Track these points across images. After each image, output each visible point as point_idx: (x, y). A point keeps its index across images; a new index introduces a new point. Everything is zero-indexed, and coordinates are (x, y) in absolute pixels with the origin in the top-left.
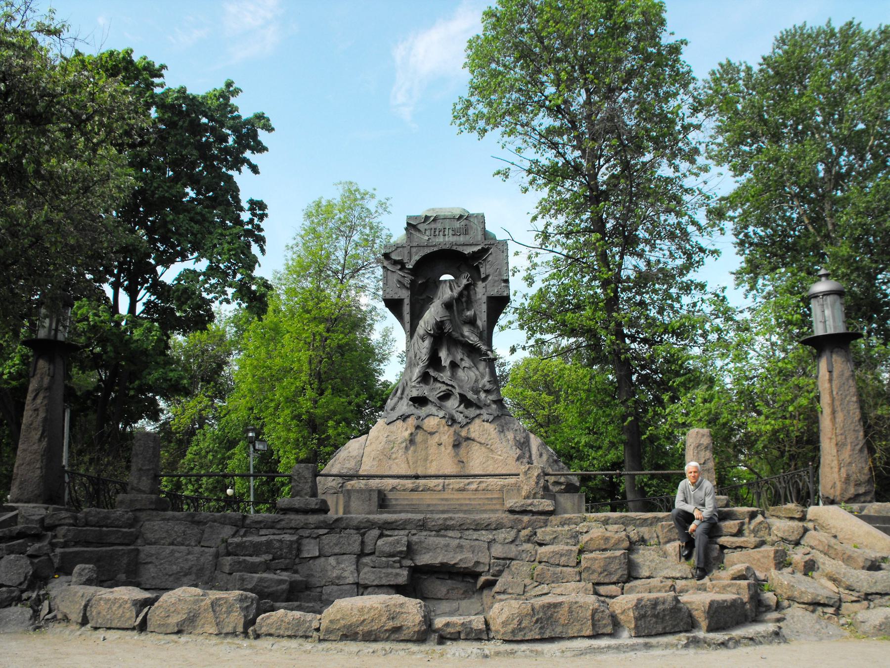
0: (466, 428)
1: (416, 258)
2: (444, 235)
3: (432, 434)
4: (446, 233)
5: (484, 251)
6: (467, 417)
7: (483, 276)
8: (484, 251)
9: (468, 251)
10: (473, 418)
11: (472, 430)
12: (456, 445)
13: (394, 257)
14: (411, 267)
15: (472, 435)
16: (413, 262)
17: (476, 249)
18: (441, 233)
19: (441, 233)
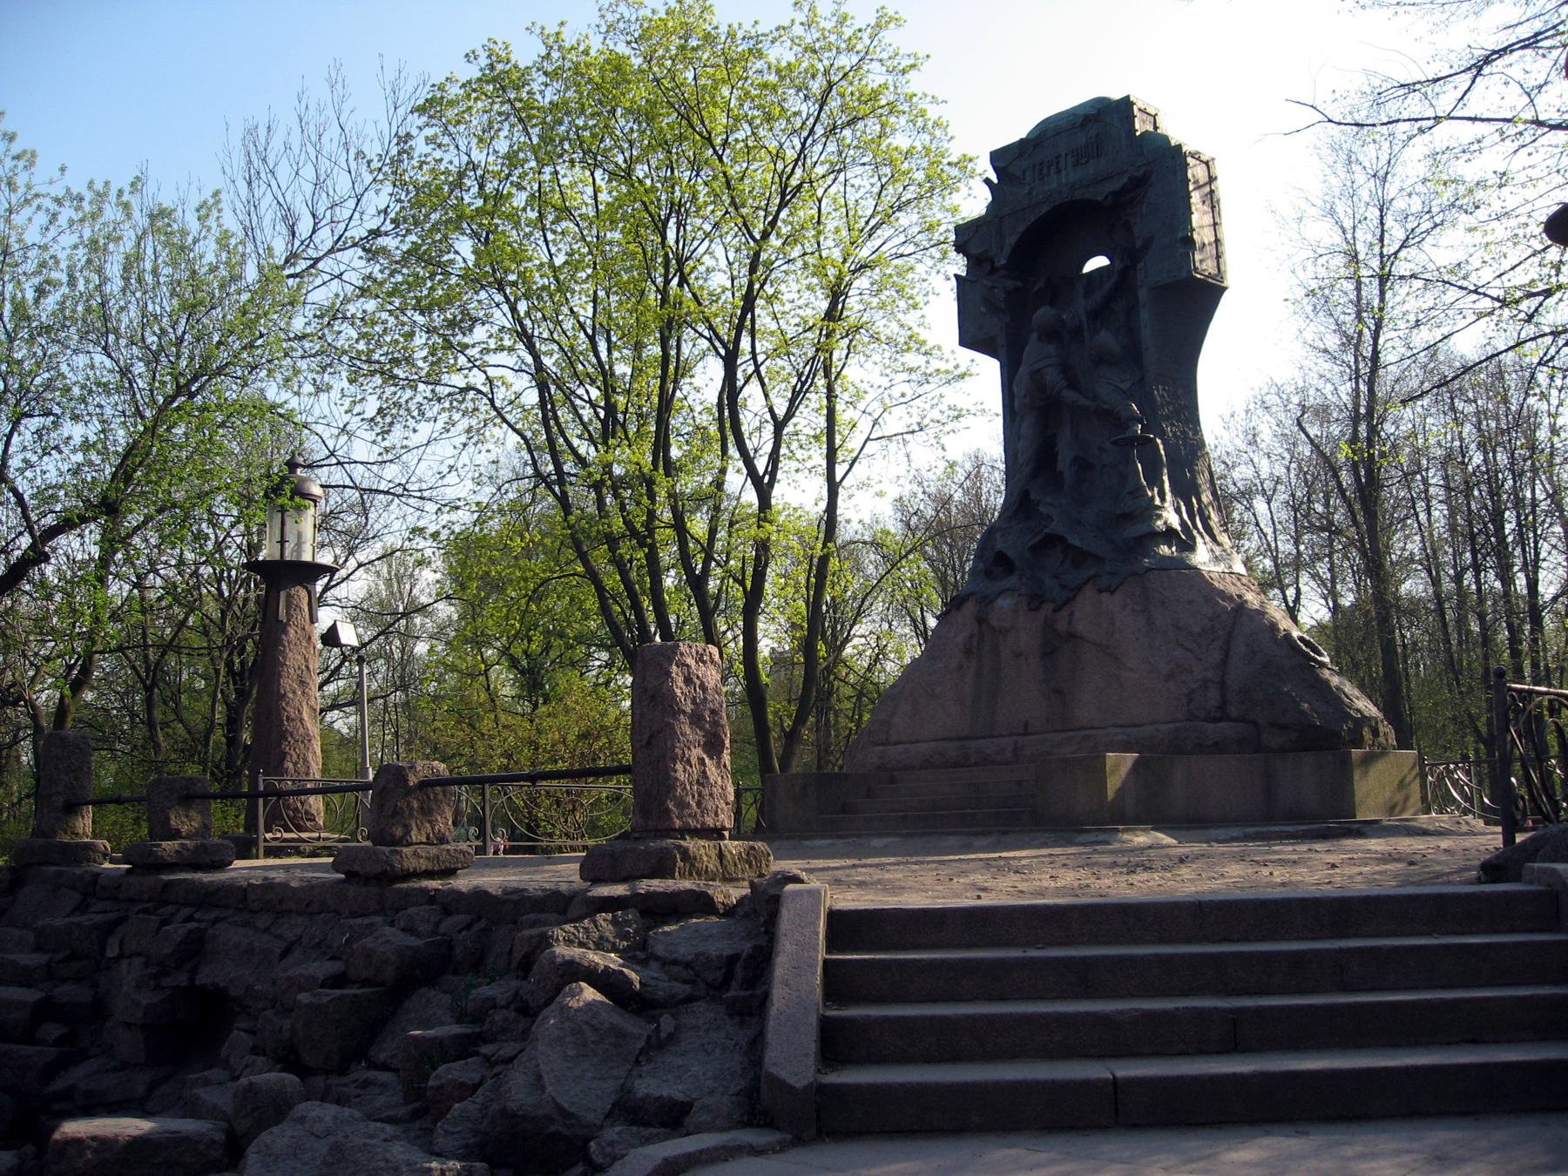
0: (1064, 613)
1: (1011, 240)
2: (1059, 172)
3: (1004, 632)
4: (1062, 166)
5: (1139, 183)
6: (1064, 587)
7: (1139, 243)
8: (1139, 183)
9: (1100, 193)
10: (1079, 588)
11: (1077, 615)
12: (1048, 653)
13: (976, 250)
14: (1003, 262)
15: (1081, 627)
16: (1007, 250)
17: (1117, 185)
18: (1053, 171)
19: (1053, 171)
